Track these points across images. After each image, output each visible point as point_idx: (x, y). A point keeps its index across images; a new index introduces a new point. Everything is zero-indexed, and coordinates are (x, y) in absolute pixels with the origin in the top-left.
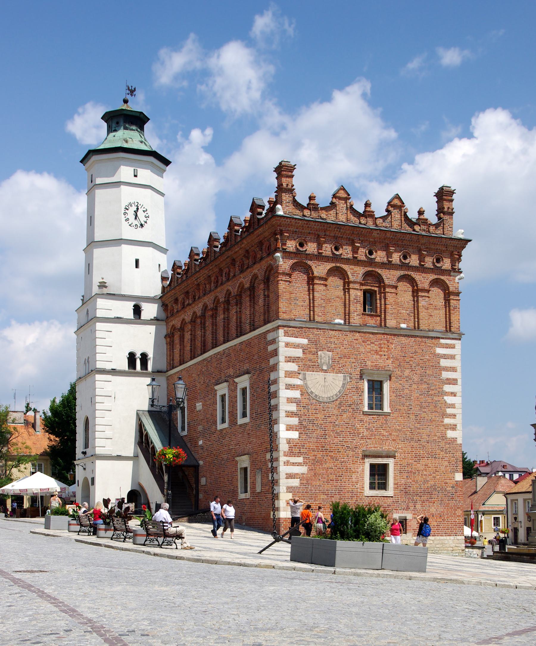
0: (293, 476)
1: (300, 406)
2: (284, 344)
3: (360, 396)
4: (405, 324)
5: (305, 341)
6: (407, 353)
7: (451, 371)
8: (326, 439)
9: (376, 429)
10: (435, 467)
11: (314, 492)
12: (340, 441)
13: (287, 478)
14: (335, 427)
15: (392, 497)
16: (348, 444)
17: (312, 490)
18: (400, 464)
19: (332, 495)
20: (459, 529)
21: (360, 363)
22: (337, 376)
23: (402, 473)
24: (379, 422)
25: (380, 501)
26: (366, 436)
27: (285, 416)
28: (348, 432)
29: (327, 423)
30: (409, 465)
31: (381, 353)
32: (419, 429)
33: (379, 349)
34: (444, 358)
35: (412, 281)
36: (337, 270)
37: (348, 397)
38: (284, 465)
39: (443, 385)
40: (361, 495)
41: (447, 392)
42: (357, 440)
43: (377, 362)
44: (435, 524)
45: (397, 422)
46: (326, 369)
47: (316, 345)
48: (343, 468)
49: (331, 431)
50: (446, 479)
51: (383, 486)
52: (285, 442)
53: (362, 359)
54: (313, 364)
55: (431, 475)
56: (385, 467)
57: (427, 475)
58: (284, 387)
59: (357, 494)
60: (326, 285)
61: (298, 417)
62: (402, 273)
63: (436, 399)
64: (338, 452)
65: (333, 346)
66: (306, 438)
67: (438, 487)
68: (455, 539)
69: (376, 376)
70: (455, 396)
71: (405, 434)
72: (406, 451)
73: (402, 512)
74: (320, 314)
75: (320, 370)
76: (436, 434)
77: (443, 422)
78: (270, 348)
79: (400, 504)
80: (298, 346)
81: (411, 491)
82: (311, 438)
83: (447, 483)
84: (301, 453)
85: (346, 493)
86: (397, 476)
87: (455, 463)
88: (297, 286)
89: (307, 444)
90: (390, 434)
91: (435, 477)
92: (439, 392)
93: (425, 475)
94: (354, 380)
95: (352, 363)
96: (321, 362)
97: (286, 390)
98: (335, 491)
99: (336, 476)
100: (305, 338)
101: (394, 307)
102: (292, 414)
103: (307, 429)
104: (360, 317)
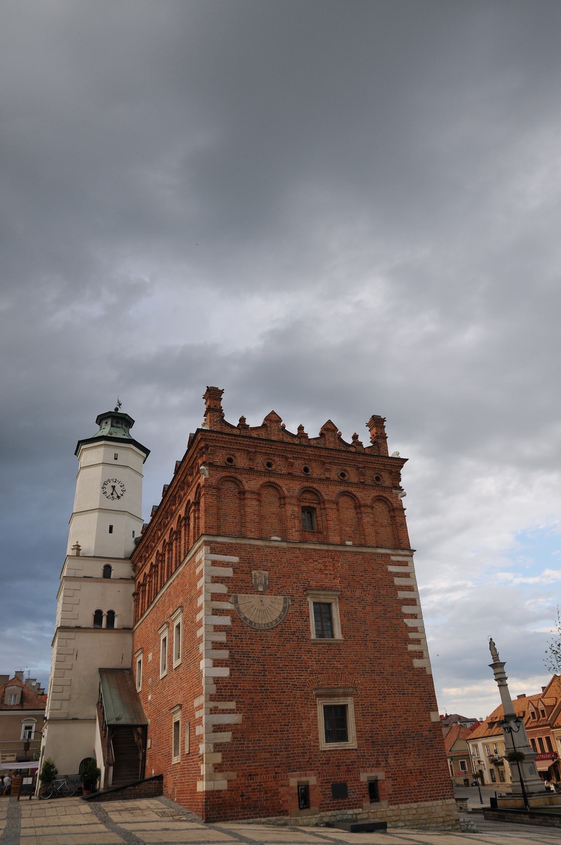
0: (222, 728)
1: (231, 636)
2: (210, 562)
3: (305, 621)
4: (350, 541)
5: (235, 559)
6: (355, 572)
7: (407, 591)
8: (266, 676)
9: (328, 661)
10: (404, 706)
11: (252, 750)
12: (283, 679)
13: (214, 731)
14: (276, 660)
15: (356, 750)
16: (295, 682)
17: (248, 747)
18: (361, 705)
19: (276, 752)
20: (447, 789)
21: (303, 583)
22: (275, 599)
23: (365, 716)
24: (331, 652)
25: (341, 756)
26: (317, 671)
27: (211, 648)
28: (294, 665)
29: (266, 655)
30: (373, 705)
31: (327, 572)
32: (380, 659)
33: (323, 568)
34: (398, 577)
35: (353, 497)
36: (271, 486)
37: (290, 623)
38: (211, 714)
39: (401, 606)
40: (315, 749)
41: (406, 614)
42: (305, 676)
43: (322, 582)
44: (415, 783)
45: (352, 652)
46: (262, 590)
47: (248, 563)
48: (289, 714)
49: (272, 665)
50: (420, 721)
51: (343, 737)
52: (211, 681)
53: (305, 579)
54: (246, 585)
55: (402, 716)
56: (344, 708)
57: (396, 717)
58: (210, 613)
59: (311, 749)
60: (259, 501)
61: (229, 649)
62: (342, 488)
63: (394, 622)
64: (281, 692)
65: (269, 564)
66: (239, 675)
67: (412, 732)
68: (444, 804)
69: (323, 597)
70: (416, 617)
71: (364, 666)
72: (367, 687)
73: (371, 770)
74: (253, 530)
75: (255, 592)
76: (400, 664)
77: (406, 649)
78: (198, 571)
79: (368, 759)
80: (227, 564)
81: (379, 739)
82: (246, 675)
83: (423, 726)
84: (233, 695)
85: (295, 748)
86: (360, 720)
87: (428, 699)
88: (226, 502)
89: (241, 683)
90: (345, 666)
91: (407, 719)
92: (397, 614)
93: (393, 717)
94: (297, 603)
95: (293, 583)
96: (255, 582)
97: (212, 616)
98: (280, 746)
99: (281, 725)
100: (235, 556)
101: (336, 523)
102: (221, 646)
103: (240, 664)
104: (299, 533)
